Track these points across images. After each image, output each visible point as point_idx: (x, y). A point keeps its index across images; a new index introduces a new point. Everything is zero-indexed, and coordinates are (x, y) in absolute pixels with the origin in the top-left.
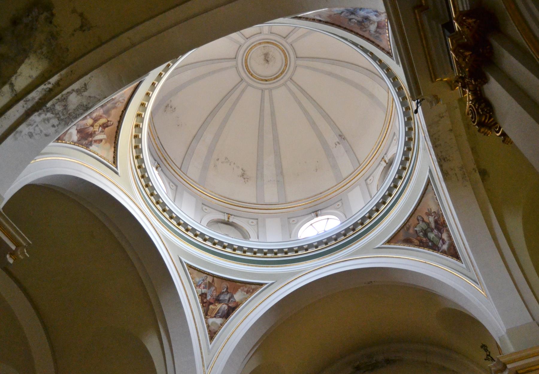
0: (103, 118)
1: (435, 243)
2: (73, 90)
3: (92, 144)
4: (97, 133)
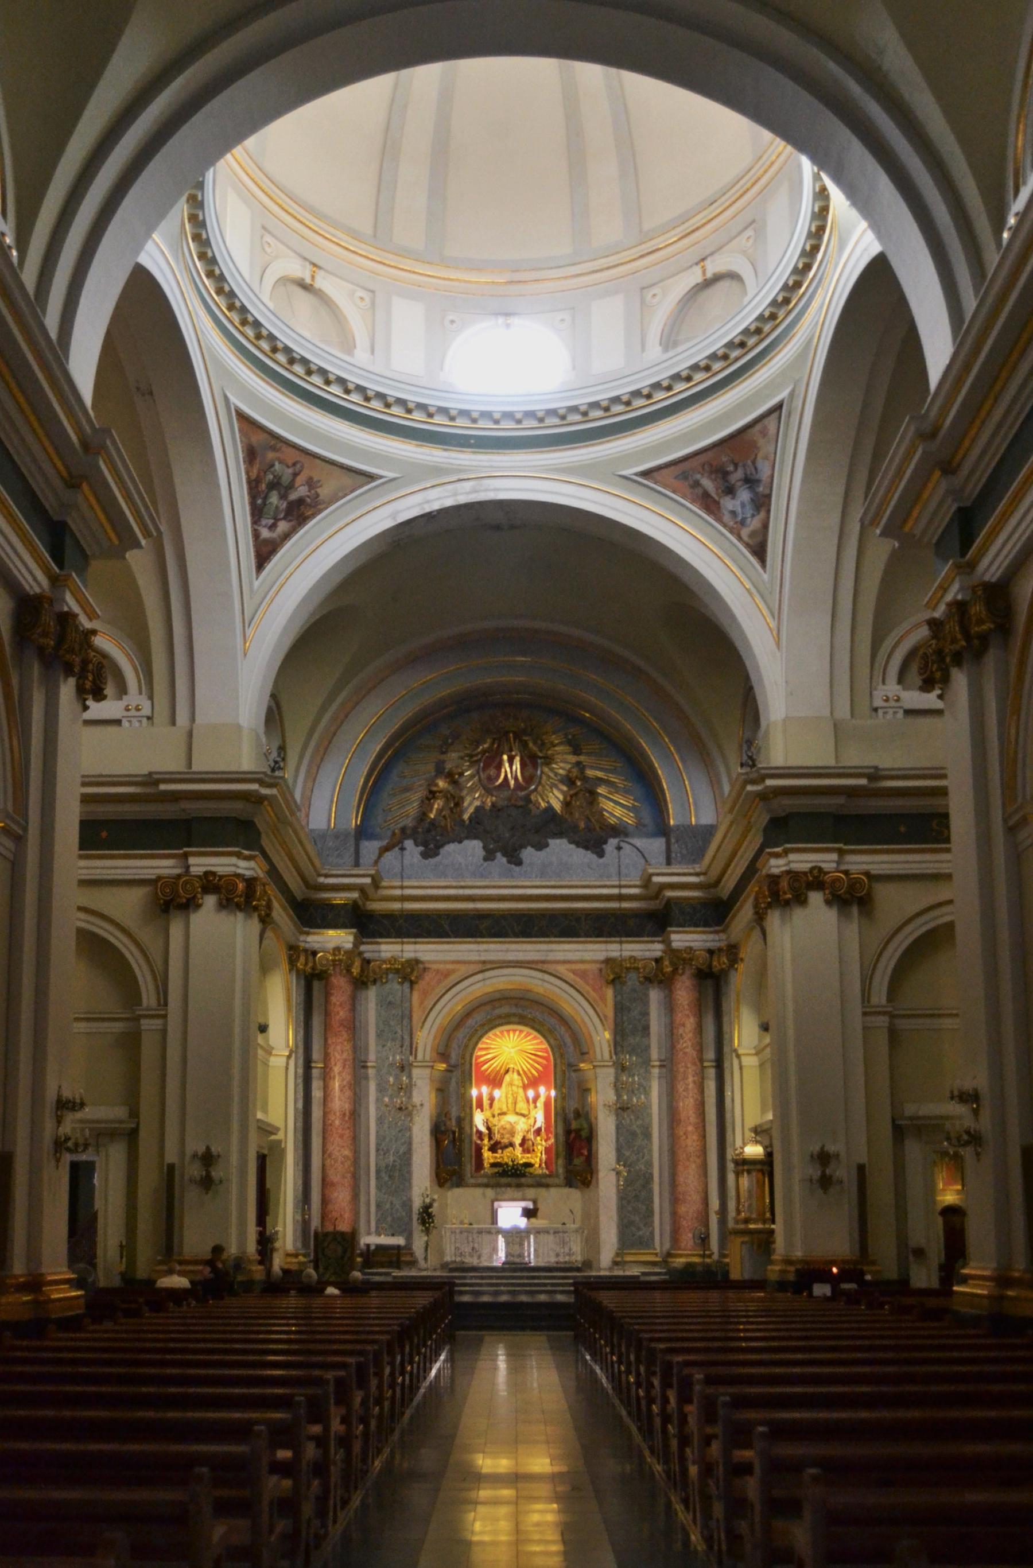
1: (265, 510)
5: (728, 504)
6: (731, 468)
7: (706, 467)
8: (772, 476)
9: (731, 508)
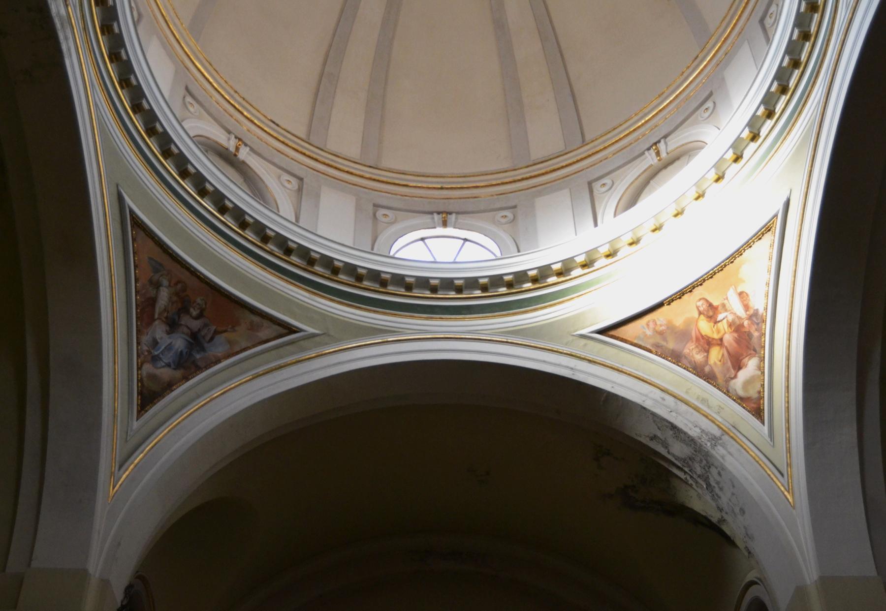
0: (699, 331)
2: (669, 452)
3: (755, 310)
4: (730, 318)
5: (159, 331)
6: (194, 313)
7: (179, 286)
8: (218, 361)
9: (158, 337)
